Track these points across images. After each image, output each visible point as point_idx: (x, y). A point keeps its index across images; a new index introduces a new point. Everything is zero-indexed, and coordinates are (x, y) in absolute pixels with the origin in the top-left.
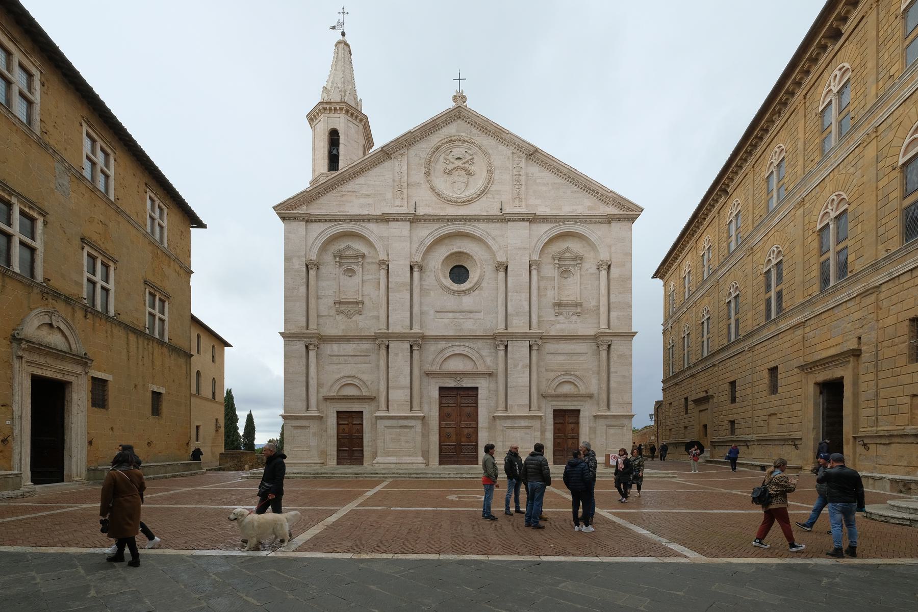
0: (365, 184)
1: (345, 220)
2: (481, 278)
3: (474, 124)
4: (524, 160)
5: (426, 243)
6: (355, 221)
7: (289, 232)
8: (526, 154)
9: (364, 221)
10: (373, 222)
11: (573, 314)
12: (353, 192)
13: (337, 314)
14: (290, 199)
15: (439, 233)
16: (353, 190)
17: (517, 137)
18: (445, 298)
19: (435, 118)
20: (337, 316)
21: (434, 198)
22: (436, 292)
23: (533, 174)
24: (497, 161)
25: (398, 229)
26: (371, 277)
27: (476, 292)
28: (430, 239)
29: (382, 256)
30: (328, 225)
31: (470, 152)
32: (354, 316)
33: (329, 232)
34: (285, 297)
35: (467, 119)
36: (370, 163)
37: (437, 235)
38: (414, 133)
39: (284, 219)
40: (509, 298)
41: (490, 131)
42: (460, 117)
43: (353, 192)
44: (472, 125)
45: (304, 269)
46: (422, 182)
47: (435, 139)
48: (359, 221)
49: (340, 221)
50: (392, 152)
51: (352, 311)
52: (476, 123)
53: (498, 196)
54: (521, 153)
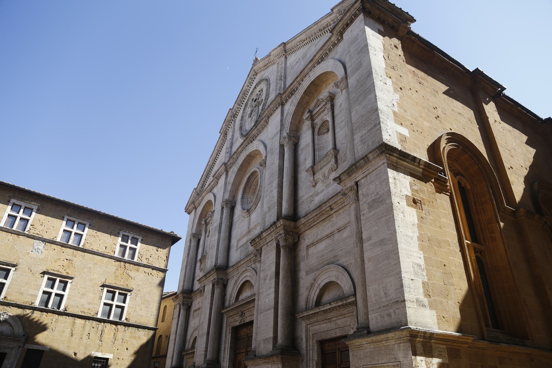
11: (329, 173)
14: (190, 199)
38: (234, 108)
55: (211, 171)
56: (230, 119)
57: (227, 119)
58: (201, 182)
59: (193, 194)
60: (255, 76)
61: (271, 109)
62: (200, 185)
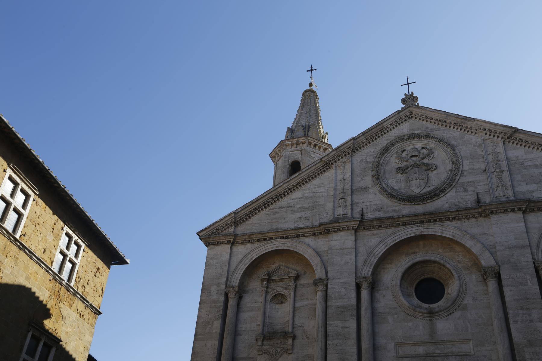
0: (302, 198)
1: (277, 238)
2: (462, 292)
3: (429, 120)
4: (501, 144)
5: (378, 252)
6: (287, 238)
7: (211, 259)
8: (502, 138)
9: (298, 236)
10: (309, 235)
12: (288, 207)
13: (259, 355)
14: (217, 222)
15: (394, 239)
16: (287, 205)
17: (485, 122)
18: (410, 324)
19: (382, 122)
20: (259, 357)
21: (386, 201)
22: (396, 316)
23: (517, 157)
24: (463, 150)
25: (339, 240)
26: (306, 303)
27: (458, 314)
28: (381, 248)
29: (319, 273)
30: (256, 245)
31: (428, 147)
32: (280, 357)
33: (256, 253)
34: (196, 335)
35: (420, 116)
36: (309, 176)
37: (390, 242)
38: (358, 140)
39: (207, 245)
40: (511, 320)
41: (451, 123)
42: (412, 117)
43: (288, 207)
44: (427, 121)
45: (222, 299)
46: (370, 186)
47: (383, 141)
48: (293, 237)
49: (271, 239)
50: (333, 162)
51: (279, 350)
52: (432, 118)
53: (471, 189)
54: (496, 137)
55: (276, 200)
56: (346, 150)
57: (342, 148)
58: (251, 207)
59: (228, 218)
60: (407, 118)
61: (504, 207)
62: (246, 211)
